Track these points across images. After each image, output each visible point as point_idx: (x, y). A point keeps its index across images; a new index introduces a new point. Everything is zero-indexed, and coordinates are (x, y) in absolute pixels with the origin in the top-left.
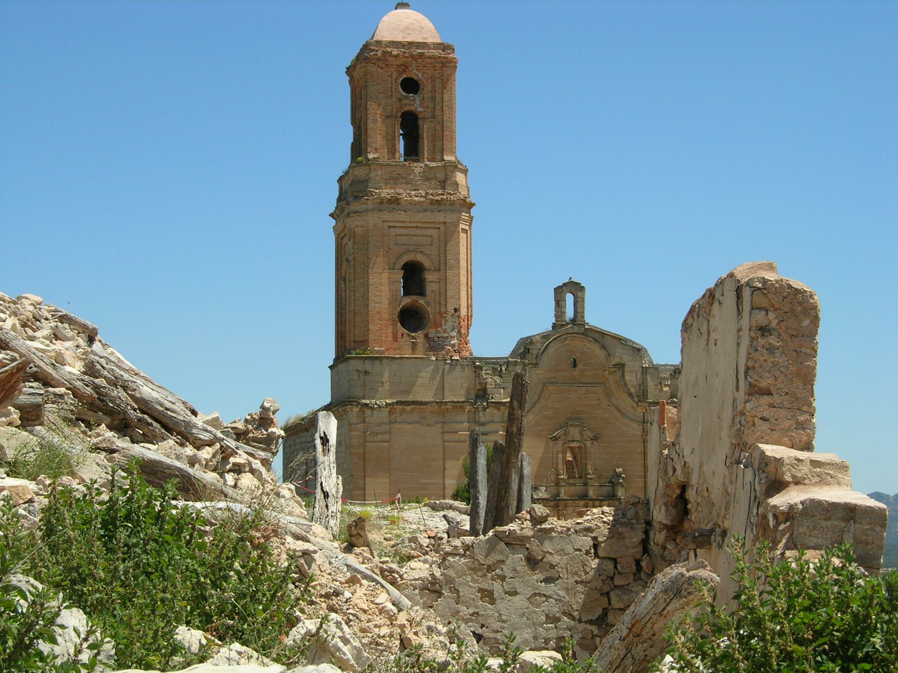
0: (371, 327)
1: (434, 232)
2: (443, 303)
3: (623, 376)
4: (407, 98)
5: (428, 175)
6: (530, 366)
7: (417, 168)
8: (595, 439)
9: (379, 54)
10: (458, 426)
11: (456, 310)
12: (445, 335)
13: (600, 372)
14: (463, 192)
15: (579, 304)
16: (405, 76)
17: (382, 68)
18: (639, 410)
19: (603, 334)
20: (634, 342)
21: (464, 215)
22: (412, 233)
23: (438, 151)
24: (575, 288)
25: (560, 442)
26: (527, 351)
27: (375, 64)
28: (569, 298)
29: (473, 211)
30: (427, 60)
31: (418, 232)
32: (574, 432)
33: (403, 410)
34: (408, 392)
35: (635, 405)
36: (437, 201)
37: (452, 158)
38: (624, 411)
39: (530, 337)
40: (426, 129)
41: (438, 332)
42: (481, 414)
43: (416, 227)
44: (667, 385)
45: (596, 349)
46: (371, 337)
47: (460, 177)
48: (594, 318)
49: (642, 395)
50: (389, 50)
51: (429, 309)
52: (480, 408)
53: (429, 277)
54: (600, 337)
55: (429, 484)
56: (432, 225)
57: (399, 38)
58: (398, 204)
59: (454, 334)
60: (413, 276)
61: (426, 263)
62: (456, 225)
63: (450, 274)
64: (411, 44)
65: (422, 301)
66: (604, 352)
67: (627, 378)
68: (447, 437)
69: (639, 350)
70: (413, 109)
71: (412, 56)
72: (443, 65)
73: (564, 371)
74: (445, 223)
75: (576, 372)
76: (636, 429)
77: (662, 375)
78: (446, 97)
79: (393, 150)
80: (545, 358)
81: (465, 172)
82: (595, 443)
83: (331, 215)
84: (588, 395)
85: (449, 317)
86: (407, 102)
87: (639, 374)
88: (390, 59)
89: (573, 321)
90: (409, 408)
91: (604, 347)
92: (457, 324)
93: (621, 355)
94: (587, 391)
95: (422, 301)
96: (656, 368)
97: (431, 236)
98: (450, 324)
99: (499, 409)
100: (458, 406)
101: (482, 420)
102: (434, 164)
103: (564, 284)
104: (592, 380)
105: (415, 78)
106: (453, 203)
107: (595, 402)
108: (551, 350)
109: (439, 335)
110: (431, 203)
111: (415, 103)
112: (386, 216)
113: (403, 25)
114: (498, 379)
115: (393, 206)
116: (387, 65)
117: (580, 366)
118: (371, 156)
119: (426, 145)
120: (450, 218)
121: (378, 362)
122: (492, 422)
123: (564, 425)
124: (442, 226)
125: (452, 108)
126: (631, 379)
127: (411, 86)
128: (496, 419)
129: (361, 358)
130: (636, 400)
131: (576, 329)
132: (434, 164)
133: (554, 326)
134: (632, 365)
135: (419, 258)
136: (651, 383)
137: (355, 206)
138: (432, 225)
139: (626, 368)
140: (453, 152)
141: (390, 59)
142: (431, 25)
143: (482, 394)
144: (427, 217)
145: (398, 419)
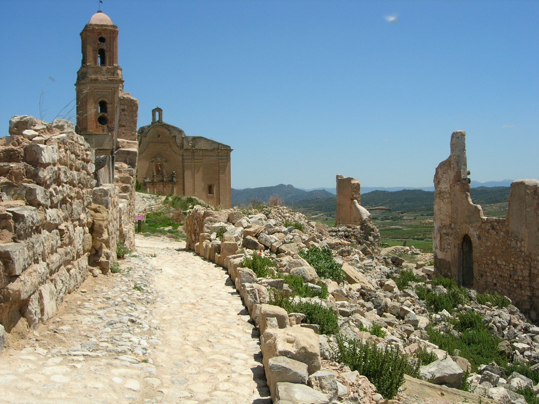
1: (110, 91)
5: (108, 71)
7: (104, 68)
8: (166, 161)
14: (120, 77)
15: (160, 115)
19: (169, 126)
21: (121, 85)
23: (112, 62)
24: (159, 110)
25: (154, 163)
26: (143, 131)
28: (157, 113)
29: (124, 84)
31: (104, 90)
32: (159, 159)
33: (100, 152)
34: (101, 146)
37: (116, 65)
40: (107, 55)
45: (166, 131)
46: (88, 127)
47: (119, 72)
48: (165, 120)
49: (182, 146)
51: (108, 117)
53: (109, 106)
54: (167, 127)
57: (98, 23)
60: (103, 105)
62: (118, 88)
64: (102, 25)
65: (106, 115)
67: (177, 141)
71: (102, 29)
75: (159, 139)
76: (180, 158)
79: (96, 62)
81: (121, 70)
89: (158, 121)
90: (102, 151)
91: (169, 130)
95: (106, 115)
96: (187, 137)
102: (110, 67)
106: (116, 81)
108: (151, 131)
111: (104, 46)
112: (93, 85)
113: (100, 18)
117: (161, 137)
118: (88, 64)
119: (107, 60)
120: (116, 86)
123: (155, 157)
125: (116, 47)
126: (178, 141)
127: (102, 40)
131: (159, 124)
132: (110, 67)
133: (152, 123)
134: (178, 136)
135: (105, 99)
136: (185, 142)
137: (82, 82)
140: (117, 63)
142: (109, 19)
144: (108, 85)
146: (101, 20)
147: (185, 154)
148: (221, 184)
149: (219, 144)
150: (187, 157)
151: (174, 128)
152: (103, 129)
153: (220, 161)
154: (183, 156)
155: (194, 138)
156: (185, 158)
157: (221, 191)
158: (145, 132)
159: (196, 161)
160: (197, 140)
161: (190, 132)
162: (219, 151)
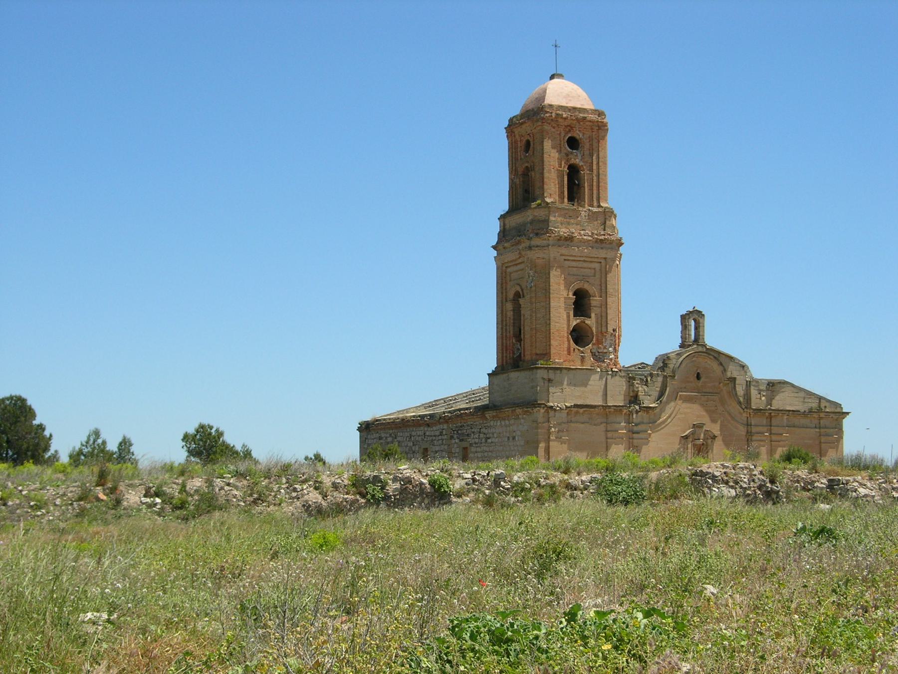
0: (552, 342)
1: (597, 266)
2: (604, 324)
3: (735, 387)
4: (572, 153)
5: (592, 216)
9: (554, 115)
10: (617, 426)
13: (717, 384)
14: (620, 235)
16: (570, 135)
18: (745, 415)
19: (719, 353)
31: (585, 265)
33: (577, 413)
39: (666, 354)
41: (599, 348)
43: (584, 261)
45: (715, 365)
46: (553, 351)
48: (711, 339)
50: (560, 113)
54: (716, 355)
56: (596, 260)
60: (581, 303)
64: (575, 108)
65: (588, 322)
66: (721, 368)
71: (578, 120)
72: (599, 128)
74: (605, 258)
78: (601, 155)
83: (494, 247)
85: (608, 336)
87: (744, 387)
88: (560, 120)
90: (581, 410)
91: (721, 364)
93: (732, 371)
96: (757, 381)
98: (608, 342)
99: (648, 412)
100: (618, 409)
105: (577, 137)
106: (611, 242)
108: (684, 365)
110: (596, 242)
112: (564, 251)
113: (563, 93)
115: (568, 243)
117: (702, 380)
121: (559, 372)
126: (740, 390)
127: (573, 143)
128: (645, 421)
129: (546, 368)
133: (682, 346)
135: (586, 286)
136: (754, 392)
138: (596, 260)
139: (737, 382)
140: (606, 200)
141: (560, 120)
145: (573, 419)
146: (567, 96)
149: (820, 398)
151: (731, 358)
152: (583, 358)
154: (748, 425)
155: (773, 386)
156: (754, 430)
161: (762, 368)
162: (822, 415)
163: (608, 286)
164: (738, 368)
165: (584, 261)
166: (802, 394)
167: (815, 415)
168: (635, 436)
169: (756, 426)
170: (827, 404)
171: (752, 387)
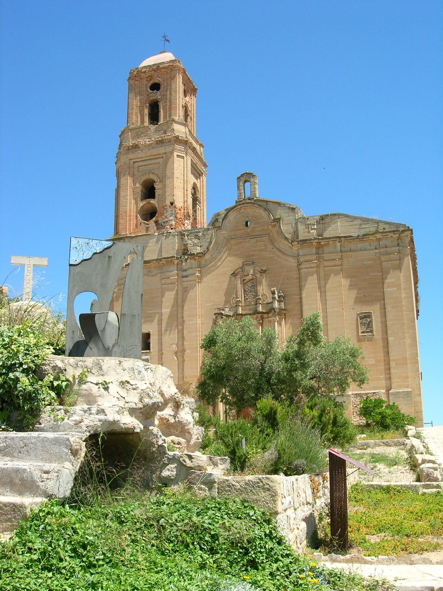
1: (160, 160)
6: (216, 229)
10: (170, 274)
11: (172, 204)
12: (166, 220)
16: (151, 82)
17: (138, 81)
18: (294, 248)
20: (290, 205)
22: (147, 164)
27: (133, 79)
30: (163, 70)
31: (151, 162)
35: (290, 245)
36: (160, 141)
38: (284, 251)
42: (184, 264)
43: (150, 159)
44: (314, 229)
45: (261, 212)
52: (183, 260)
55: (153, 313)
58: (138, 148)
59: (171, 218)
61: (155, 178)
62: (172, 153)
63: (168, 182)
68: (163, 281)
69: (293, 209)
70: (155, 98)
73: (241, 230)
75: (249, 230)
76: (293, 262)
77: (309, 222)
78: (173, 87)
79: (142, 121)
80: (226, 222)
82: (264, 275)
84: (258, 243)
86: (152, 95)
92: (173, 212)
94: (257, 240)
97: (159, 163)
98: (169, 212)
99: (195, 260)
100: (170, 260)
101: (185, 268)
103: (242, 176)
104: (260, 233)
105: (158, 82)
107: (263, 247)
108: (232, 216)
109: (164, 221)
110: (157, 144)
112: (131, 156)
114: (196, 241)
115: (134, 150)
116: (141, 79)
120: (168, 149)
121: (122, 241)
122: (192, 268)
124: (164, 156)
126: (286, 228)
127: (156, 87)
128: (194, 266)
130: (291, 242)
135: (152, 177)
136: (301, 228)
141: (142, 75)
143: (185, 251)
144: (155, 151)
147: (301, 253)
148: (388, 309)
149: (378, 222)
150: (306, 258)
152: (147, 228)
153: (383, 259)
156: (302, 259)
157: (389, 324)
158: (220, 220)
159: (326, 264)
160: (327, 220)
162: (379, 236)
163: (167, 172)
164: (287, 210)
165: (150, 159)
166: (358, 222)
167: (371, 237)
168: (184, 279)
169: (304, 255)
170: (386, 226)
171: (299, 224)
